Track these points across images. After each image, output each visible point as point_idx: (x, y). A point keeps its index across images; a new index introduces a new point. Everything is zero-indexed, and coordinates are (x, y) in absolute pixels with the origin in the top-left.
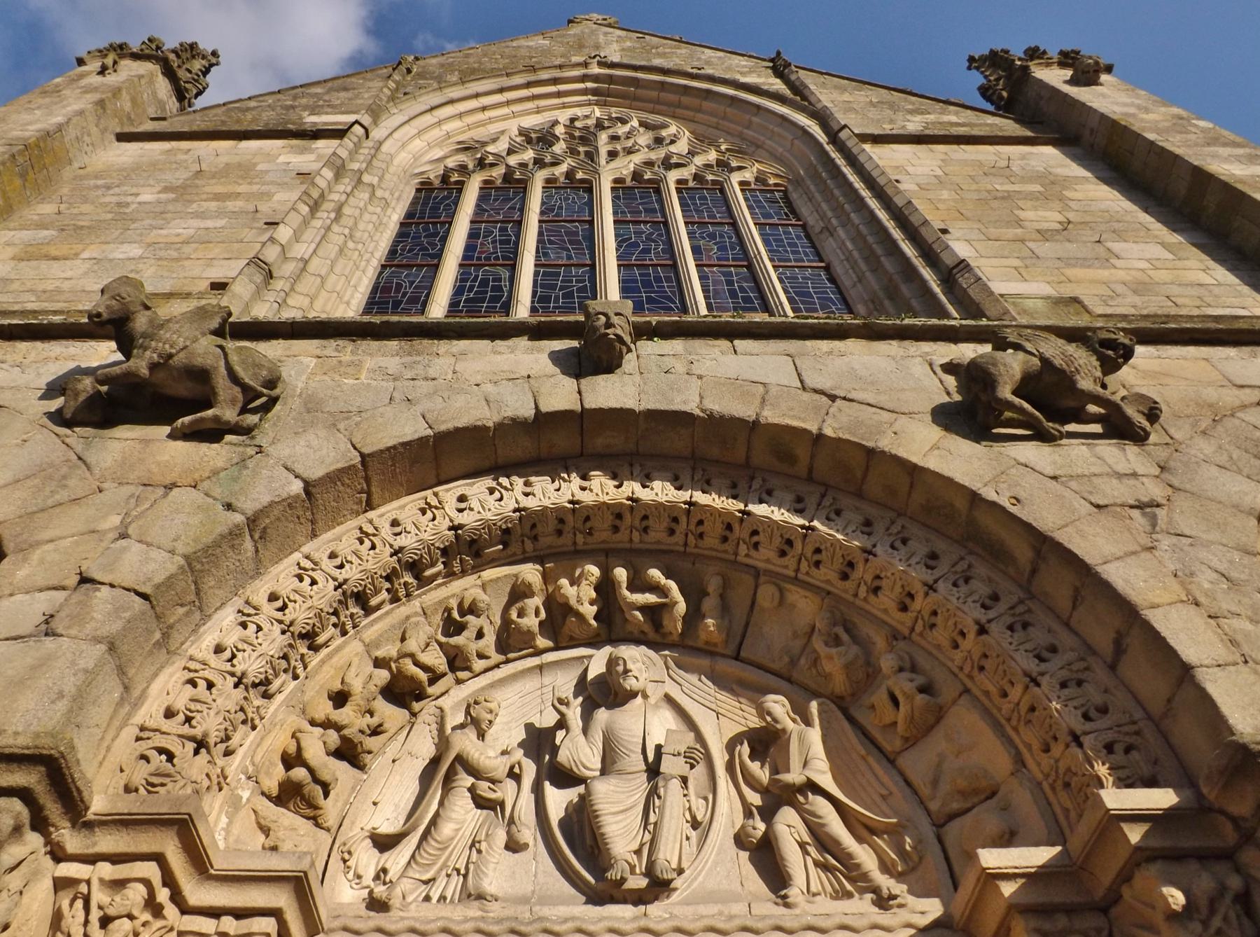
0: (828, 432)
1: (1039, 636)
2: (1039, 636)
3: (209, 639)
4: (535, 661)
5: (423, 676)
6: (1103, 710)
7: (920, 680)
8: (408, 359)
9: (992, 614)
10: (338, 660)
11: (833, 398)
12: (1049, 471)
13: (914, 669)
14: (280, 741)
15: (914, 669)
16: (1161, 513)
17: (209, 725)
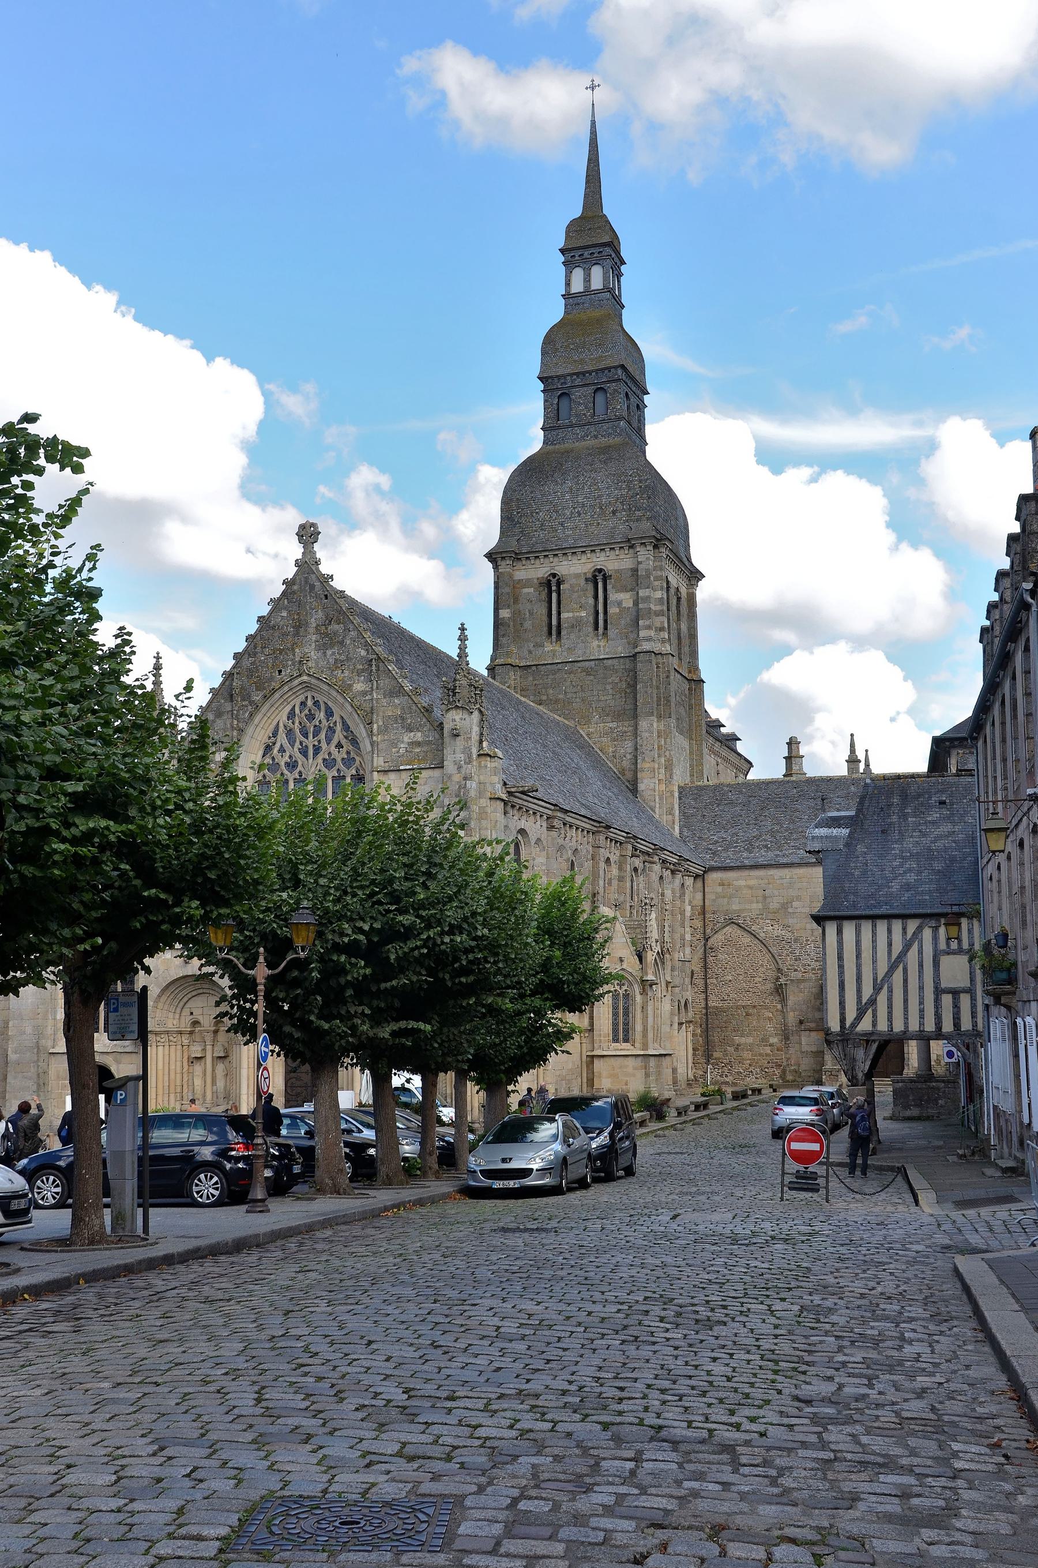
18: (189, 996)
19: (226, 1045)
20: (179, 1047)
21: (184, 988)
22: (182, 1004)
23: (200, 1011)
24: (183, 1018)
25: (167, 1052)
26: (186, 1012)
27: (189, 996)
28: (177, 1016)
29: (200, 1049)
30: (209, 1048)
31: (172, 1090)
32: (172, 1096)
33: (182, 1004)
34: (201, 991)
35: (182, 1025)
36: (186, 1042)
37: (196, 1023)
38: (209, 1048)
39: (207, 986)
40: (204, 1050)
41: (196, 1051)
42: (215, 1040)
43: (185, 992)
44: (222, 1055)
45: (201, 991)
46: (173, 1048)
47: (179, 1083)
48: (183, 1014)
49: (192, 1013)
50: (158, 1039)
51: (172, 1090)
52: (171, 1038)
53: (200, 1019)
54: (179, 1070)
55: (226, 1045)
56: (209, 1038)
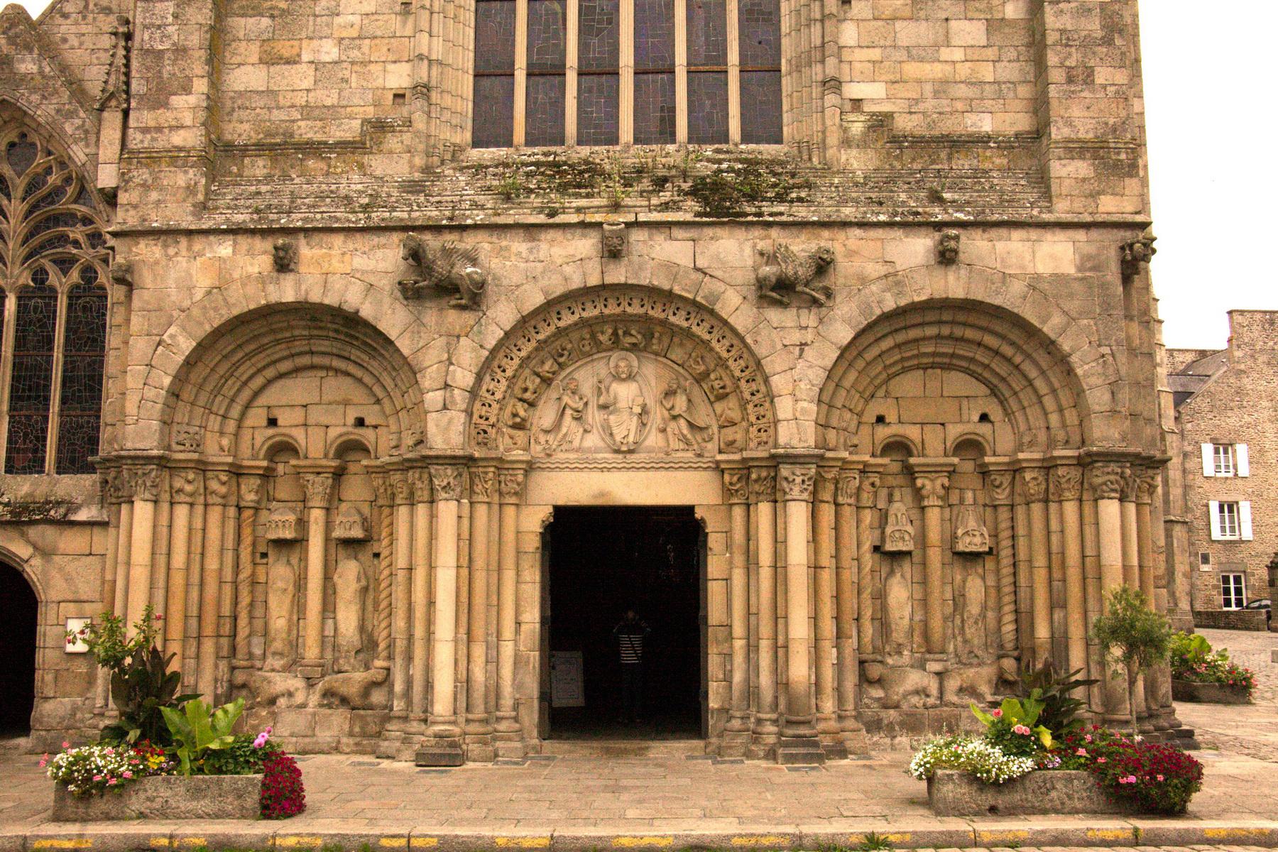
0: (698, 299)
1: (754, 386)
2: (754, 386)
3: (484, 388)
4: (590, 358)
5: (550, 375)
6: (763, 417)
7: (722, 384)
8: (529, 245)
9: (743, 374)
10: (522, 377)
11: (705, 274)
12: (775, 325)
13: (721, 379)
14: (509, 410)
15: (721, 379)
16: (806, 348)
17: (493, 420)
18: (270, 373)
19: (366, 510)
20: (232, 512)
21: (261, 349)
22: (246, 394)
23: (298, 416)
24: (246, 435)
25: (198, 524)
26: (257, 417)
27: (270, 373)
28: (231, 426)
29: (292, 518)
30: (316, 516)
31: (209, 629)
32: (208, 646)
33: (246, 394)
34: (306, 360)
35: (245, 450)
36: (250, 498)
37: (283, 449)
38: (316, 516)
39: (324, 346)
40: (302, 523)
41: (280, 523)
42: (333, 501)
43: (260, 360)
44: (357, 533)
45: (306, 360)
46: (215, 515)
47: (226, 610)
48: (249, 422)
49: (273, 422)
50: (178, 483)
51: (209, 629)
52: (214, 485)
53: (299, 435)
54: (228, 576)
55: (366, 510)
56: (318, 487)
